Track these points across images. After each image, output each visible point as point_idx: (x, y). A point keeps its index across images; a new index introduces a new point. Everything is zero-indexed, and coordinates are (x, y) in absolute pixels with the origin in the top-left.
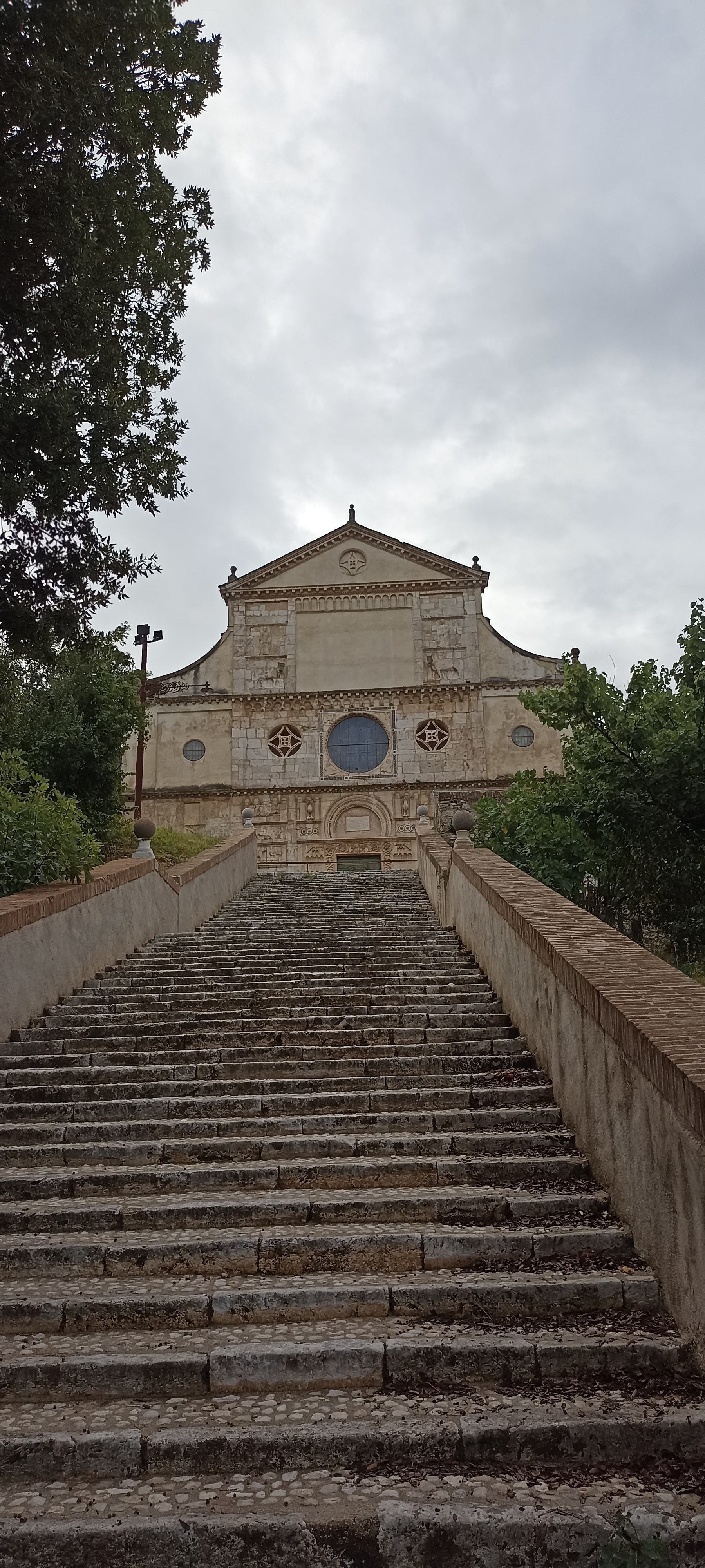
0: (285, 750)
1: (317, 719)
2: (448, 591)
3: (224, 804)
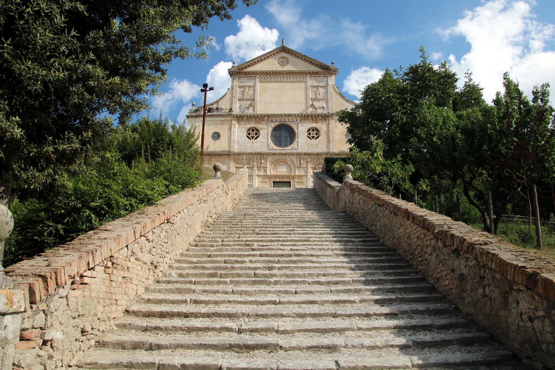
0: (253, 137)
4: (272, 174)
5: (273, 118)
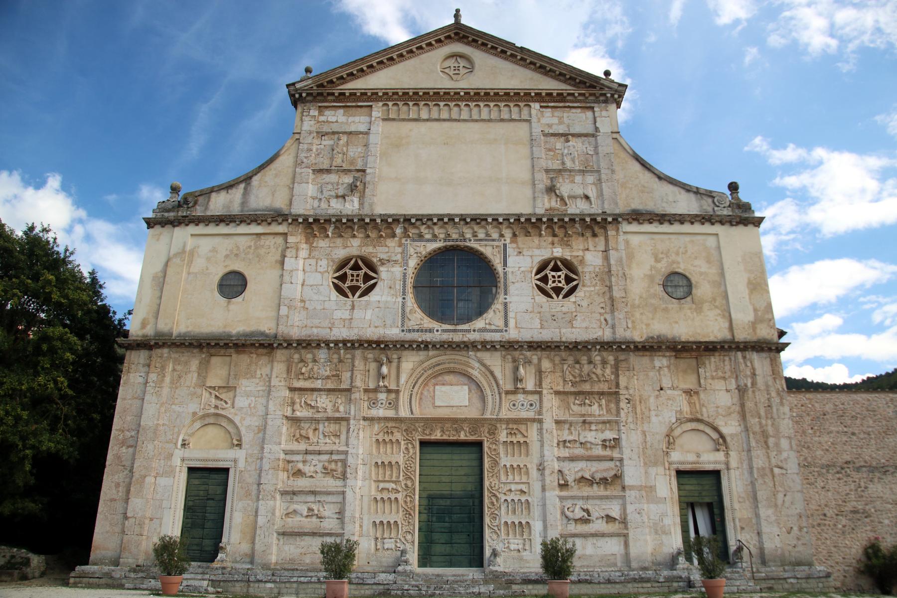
0: (354, 289)
2: (576, 105)
3: (264, 360)
4: (417, 414)
5: (423, 229)
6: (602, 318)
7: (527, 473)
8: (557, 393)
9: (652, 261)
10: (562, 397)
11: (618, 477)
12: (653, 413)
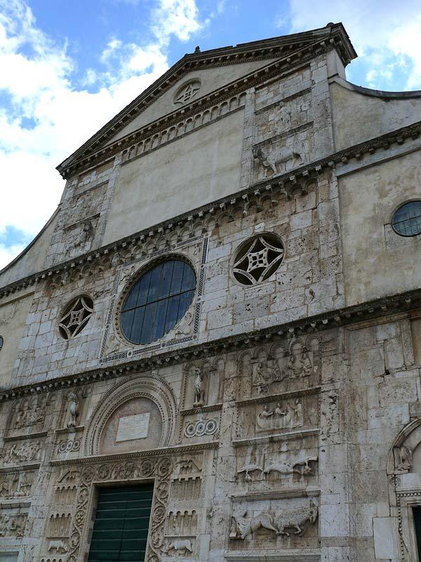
1: (113, 278)
6: (307, 291)
7: (195, 523)
8: (241, 405)
9: (375, 198)
10: (248, 409)
11: (312, 523)
12: (373, 413)
